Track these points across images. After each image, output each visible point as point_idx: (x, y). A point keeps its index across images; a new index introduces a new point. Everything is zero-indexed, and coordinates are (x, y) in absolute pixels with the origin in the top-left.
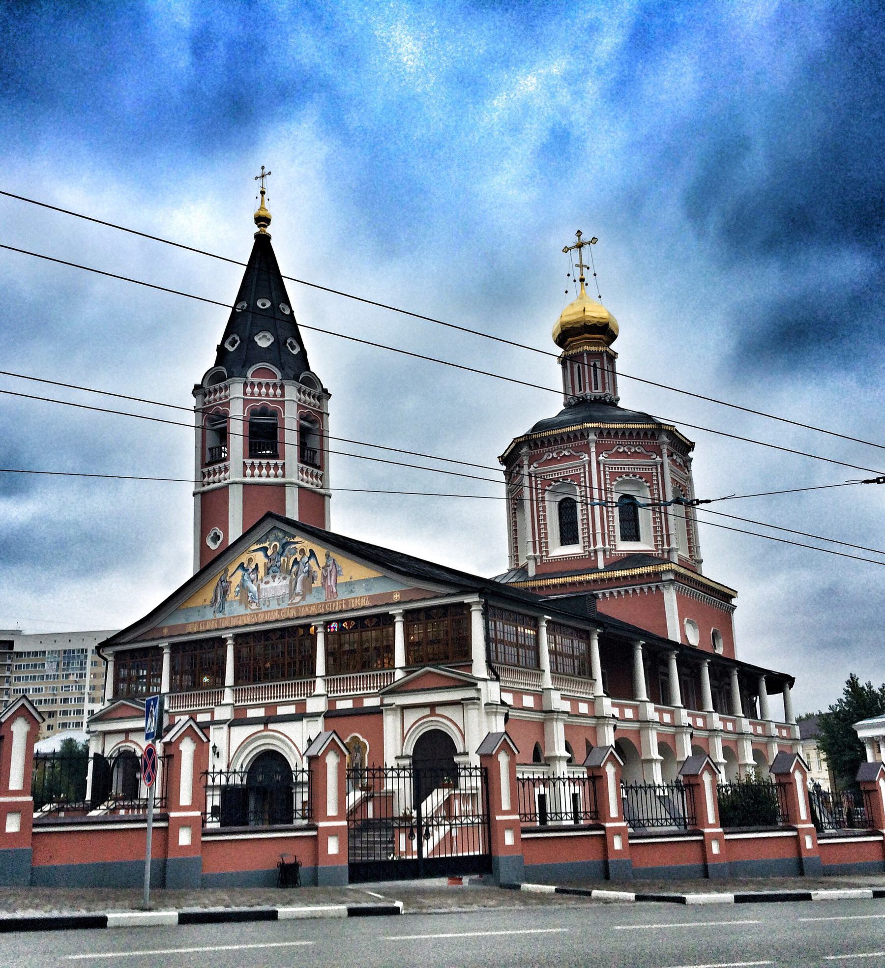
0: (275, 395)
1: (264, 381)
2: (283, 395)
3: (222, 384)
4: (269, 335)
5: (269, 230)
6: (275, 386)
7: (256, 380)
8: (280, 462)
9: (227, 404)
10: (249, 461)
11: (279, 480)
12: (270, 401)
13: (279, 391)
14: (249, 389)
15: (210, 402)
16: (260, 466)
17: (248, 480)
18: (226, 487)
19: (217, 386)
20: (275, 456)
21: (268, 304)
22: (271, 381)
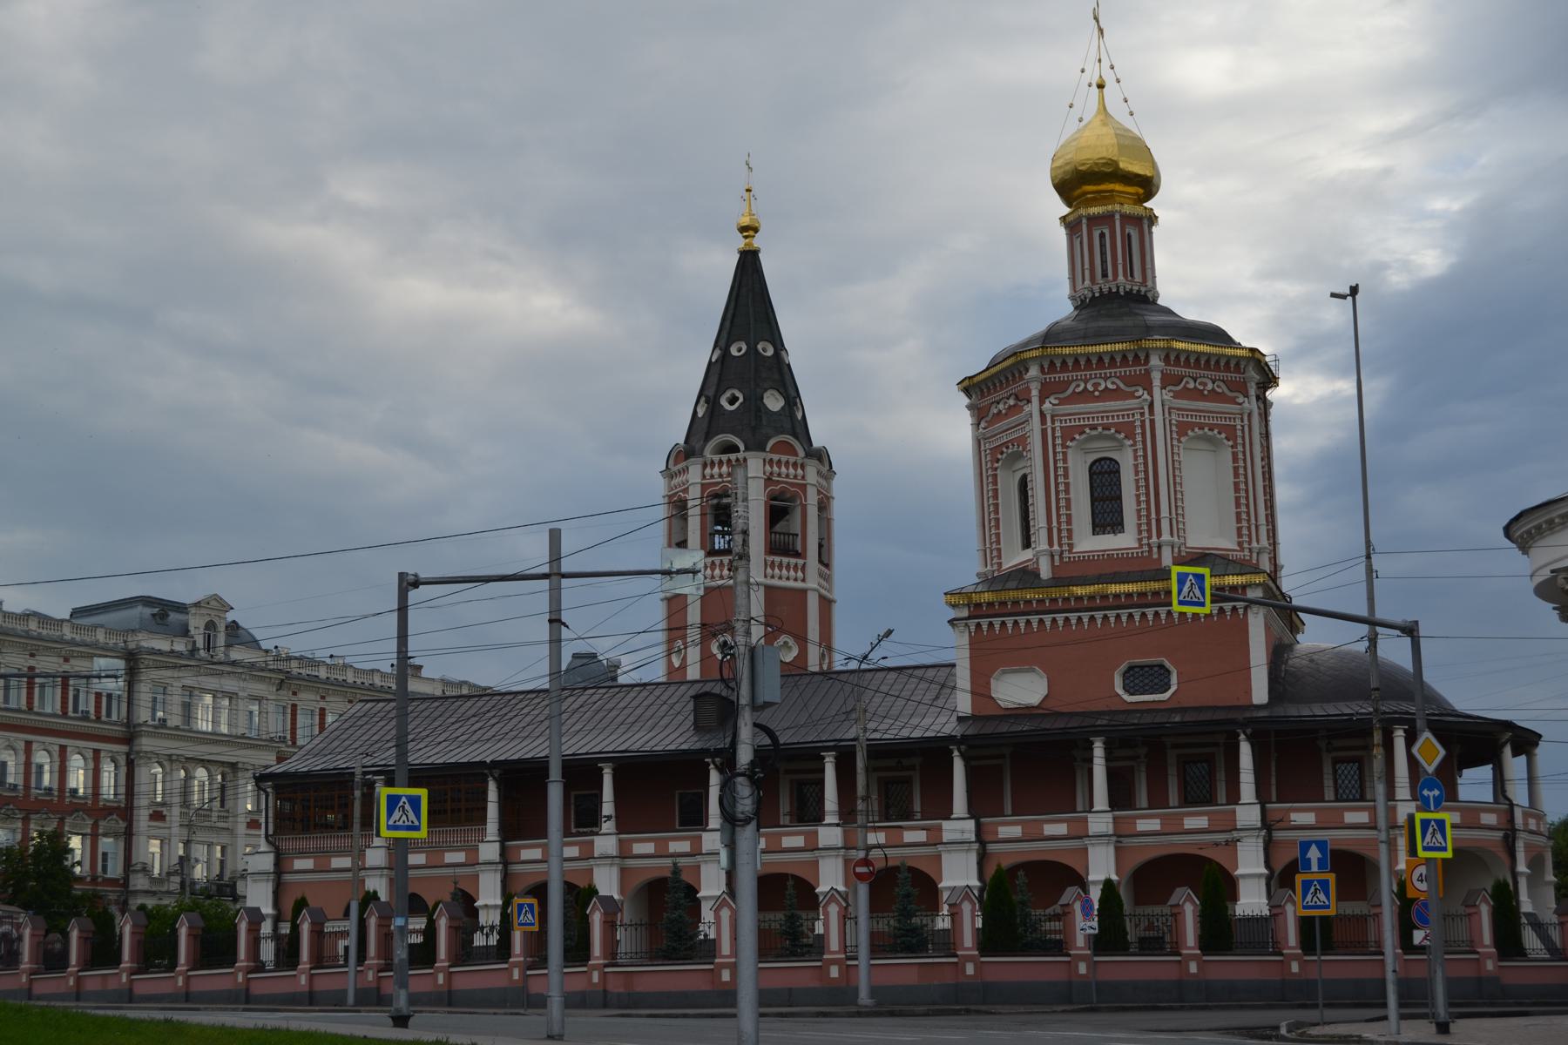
0: (795, 477)
1: (784, 458)
2: (803, 478)
3: (733, 456)
5: (757, 242)
6: (795, 465)
7: (776, 457)
8: (801, 562)
10: (770, 558)
11: (799, 585)
12: (793, 485)
13: (800, 471)
14: (768, 468)
15: (712, 476)
16: (780, 566)
17: (770, 582)
19: (724, 457)
20: (797, 555)
21: (770, 352)
22: (792, 459)
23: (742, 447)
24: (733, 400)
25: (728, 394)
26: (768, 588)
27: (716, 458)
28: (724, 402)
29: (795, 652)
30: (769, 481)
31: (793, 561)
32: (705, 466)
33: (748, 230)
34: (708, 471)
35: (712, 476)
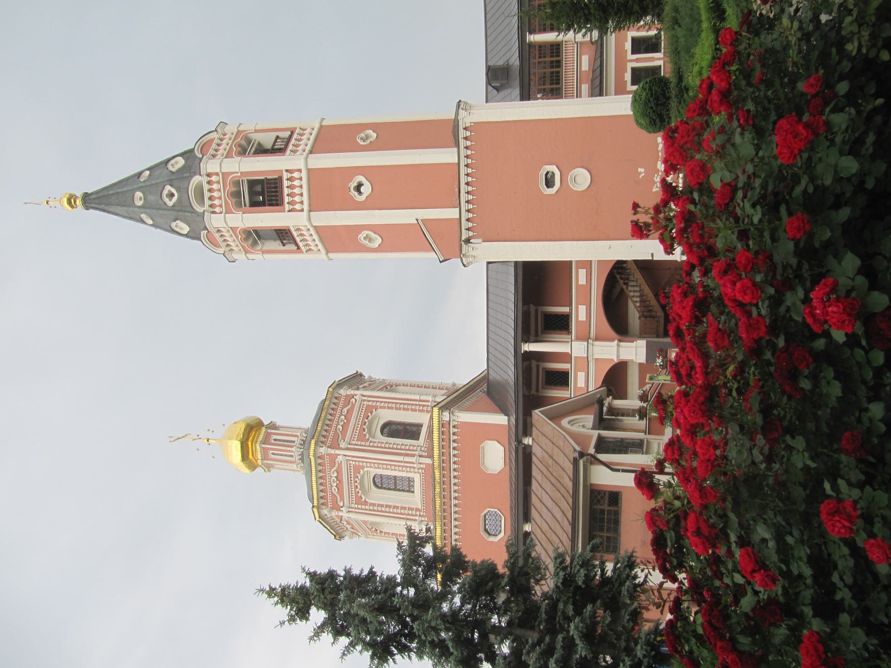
1: (214, 146)
3: (206, 187)
4: (173, 162)
5: (79, 194)
7: (211, 152)
8: (298, 131)
9: (225, 175)
10: (288, 152)
18: (309, 171)
19: (207, 195)
20: (292, 133)
21: (148, 173)
23: (196, 179)
24: (171, 195)
25: (166, 200)
26: (311, 152)
27: (207, 202)
28: (170, 203)
29: (370, 132)
30: (229, 155)
31: (295, 136)
32: (214, 212)
33: (71, 200)
34: (217, 210)
35: (221, 206)
